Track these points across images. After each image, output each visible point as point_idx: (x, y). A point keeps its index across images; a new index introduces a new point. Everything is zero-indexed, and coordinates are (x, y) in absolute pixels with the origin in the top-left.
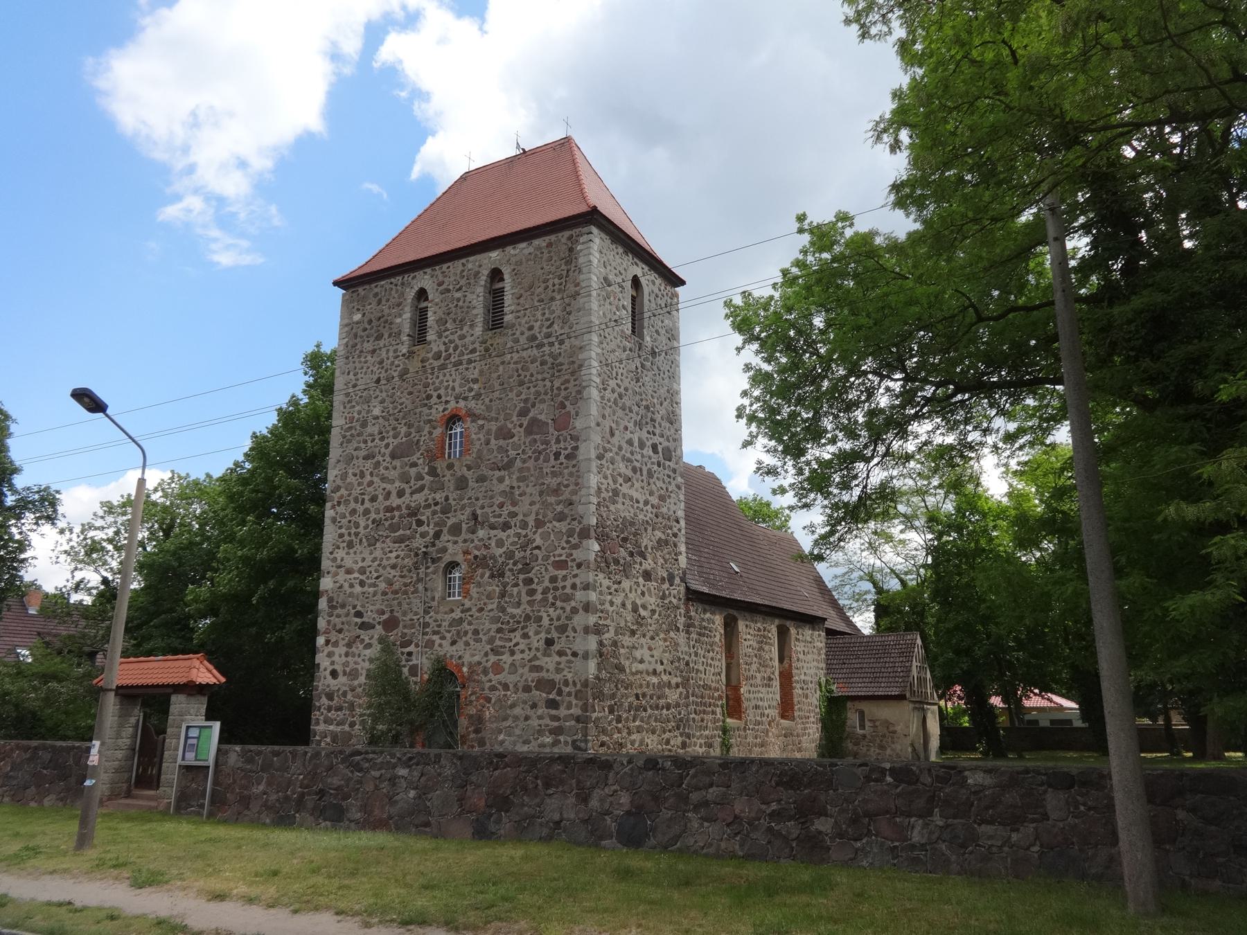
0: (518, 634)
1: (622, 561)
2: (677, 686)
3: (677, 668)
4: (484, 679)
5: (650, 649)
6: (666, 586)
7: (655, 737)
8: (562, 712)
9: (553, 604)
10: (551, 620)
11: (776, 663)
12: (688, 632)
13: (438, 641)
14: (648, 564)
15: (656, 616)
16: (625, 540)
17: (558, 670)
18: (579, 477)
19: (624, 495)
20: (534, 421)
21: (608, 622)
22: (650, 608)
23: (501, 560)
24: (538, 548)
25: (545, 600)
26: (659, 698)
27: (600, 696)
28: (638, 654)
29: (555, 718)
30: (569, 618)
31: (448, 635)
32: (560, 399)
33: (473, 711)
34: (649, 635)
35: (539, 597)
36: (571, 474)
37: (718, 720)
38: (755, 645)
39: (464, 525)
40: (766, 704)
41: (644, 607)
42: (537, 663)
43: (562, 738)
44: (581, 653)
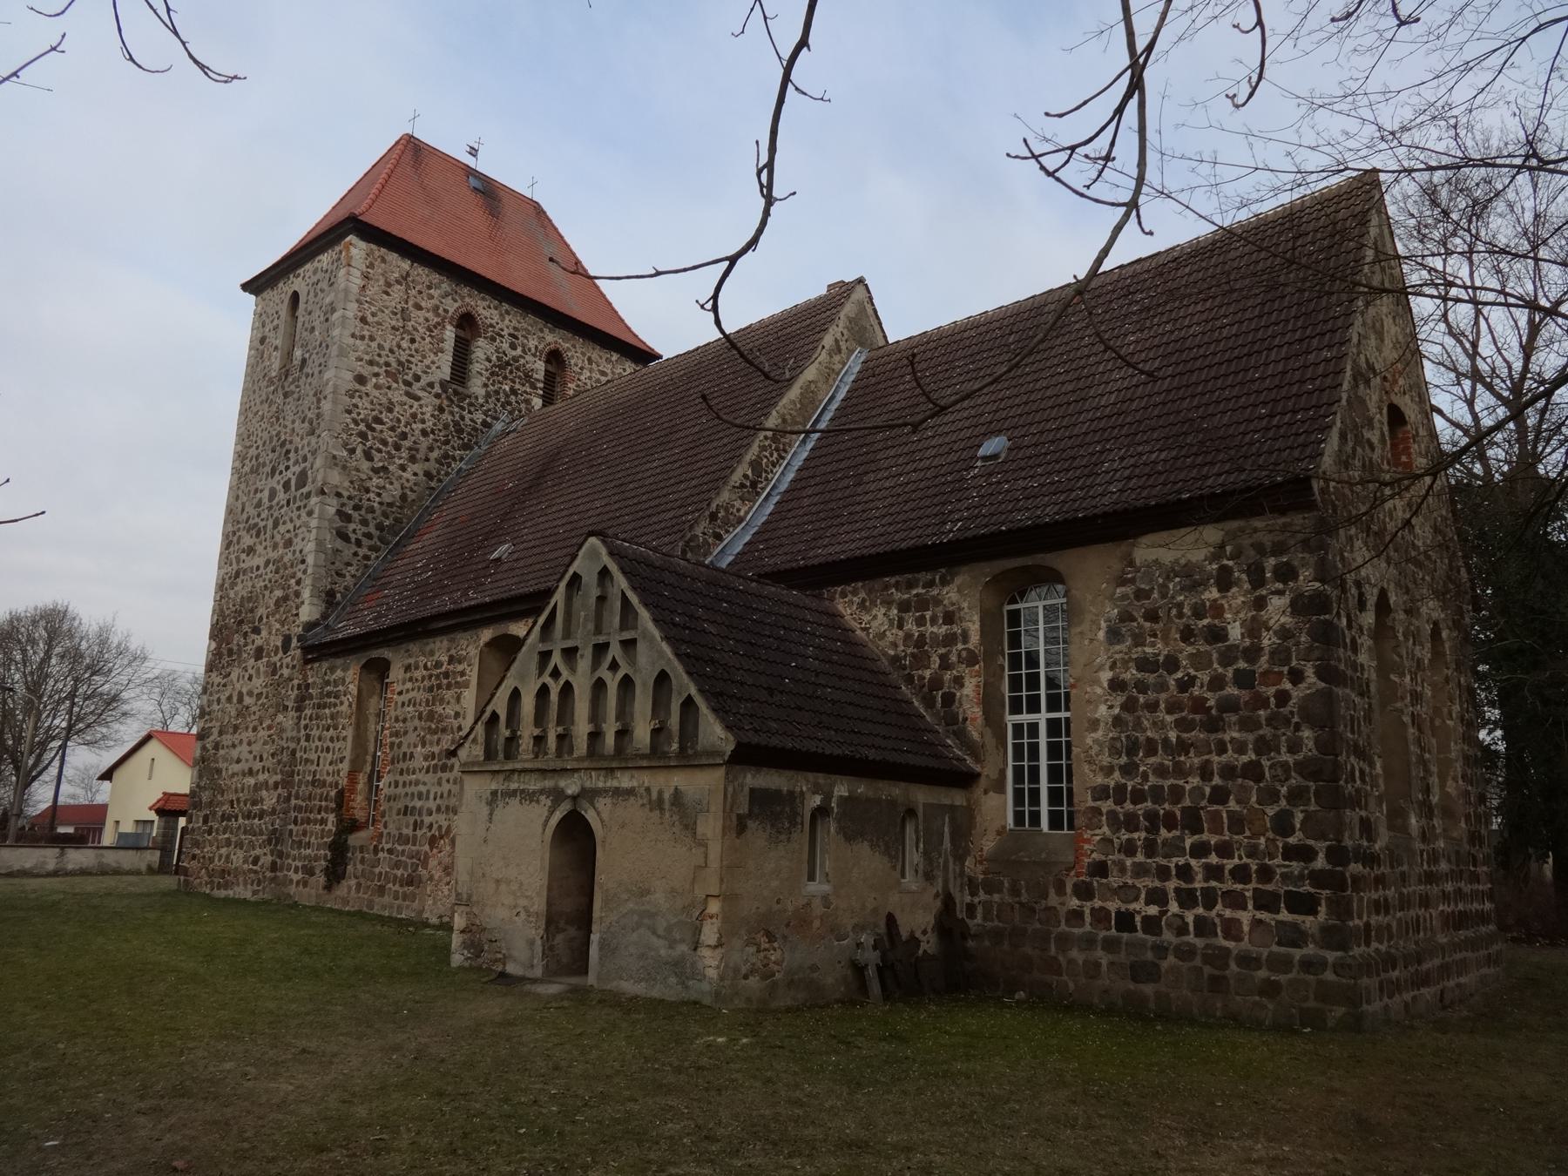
7: (241, 854)
15: (263, 700)
26: (254, 803)
38: (420, 696)
40: (432, 805)
41: (250, 693)
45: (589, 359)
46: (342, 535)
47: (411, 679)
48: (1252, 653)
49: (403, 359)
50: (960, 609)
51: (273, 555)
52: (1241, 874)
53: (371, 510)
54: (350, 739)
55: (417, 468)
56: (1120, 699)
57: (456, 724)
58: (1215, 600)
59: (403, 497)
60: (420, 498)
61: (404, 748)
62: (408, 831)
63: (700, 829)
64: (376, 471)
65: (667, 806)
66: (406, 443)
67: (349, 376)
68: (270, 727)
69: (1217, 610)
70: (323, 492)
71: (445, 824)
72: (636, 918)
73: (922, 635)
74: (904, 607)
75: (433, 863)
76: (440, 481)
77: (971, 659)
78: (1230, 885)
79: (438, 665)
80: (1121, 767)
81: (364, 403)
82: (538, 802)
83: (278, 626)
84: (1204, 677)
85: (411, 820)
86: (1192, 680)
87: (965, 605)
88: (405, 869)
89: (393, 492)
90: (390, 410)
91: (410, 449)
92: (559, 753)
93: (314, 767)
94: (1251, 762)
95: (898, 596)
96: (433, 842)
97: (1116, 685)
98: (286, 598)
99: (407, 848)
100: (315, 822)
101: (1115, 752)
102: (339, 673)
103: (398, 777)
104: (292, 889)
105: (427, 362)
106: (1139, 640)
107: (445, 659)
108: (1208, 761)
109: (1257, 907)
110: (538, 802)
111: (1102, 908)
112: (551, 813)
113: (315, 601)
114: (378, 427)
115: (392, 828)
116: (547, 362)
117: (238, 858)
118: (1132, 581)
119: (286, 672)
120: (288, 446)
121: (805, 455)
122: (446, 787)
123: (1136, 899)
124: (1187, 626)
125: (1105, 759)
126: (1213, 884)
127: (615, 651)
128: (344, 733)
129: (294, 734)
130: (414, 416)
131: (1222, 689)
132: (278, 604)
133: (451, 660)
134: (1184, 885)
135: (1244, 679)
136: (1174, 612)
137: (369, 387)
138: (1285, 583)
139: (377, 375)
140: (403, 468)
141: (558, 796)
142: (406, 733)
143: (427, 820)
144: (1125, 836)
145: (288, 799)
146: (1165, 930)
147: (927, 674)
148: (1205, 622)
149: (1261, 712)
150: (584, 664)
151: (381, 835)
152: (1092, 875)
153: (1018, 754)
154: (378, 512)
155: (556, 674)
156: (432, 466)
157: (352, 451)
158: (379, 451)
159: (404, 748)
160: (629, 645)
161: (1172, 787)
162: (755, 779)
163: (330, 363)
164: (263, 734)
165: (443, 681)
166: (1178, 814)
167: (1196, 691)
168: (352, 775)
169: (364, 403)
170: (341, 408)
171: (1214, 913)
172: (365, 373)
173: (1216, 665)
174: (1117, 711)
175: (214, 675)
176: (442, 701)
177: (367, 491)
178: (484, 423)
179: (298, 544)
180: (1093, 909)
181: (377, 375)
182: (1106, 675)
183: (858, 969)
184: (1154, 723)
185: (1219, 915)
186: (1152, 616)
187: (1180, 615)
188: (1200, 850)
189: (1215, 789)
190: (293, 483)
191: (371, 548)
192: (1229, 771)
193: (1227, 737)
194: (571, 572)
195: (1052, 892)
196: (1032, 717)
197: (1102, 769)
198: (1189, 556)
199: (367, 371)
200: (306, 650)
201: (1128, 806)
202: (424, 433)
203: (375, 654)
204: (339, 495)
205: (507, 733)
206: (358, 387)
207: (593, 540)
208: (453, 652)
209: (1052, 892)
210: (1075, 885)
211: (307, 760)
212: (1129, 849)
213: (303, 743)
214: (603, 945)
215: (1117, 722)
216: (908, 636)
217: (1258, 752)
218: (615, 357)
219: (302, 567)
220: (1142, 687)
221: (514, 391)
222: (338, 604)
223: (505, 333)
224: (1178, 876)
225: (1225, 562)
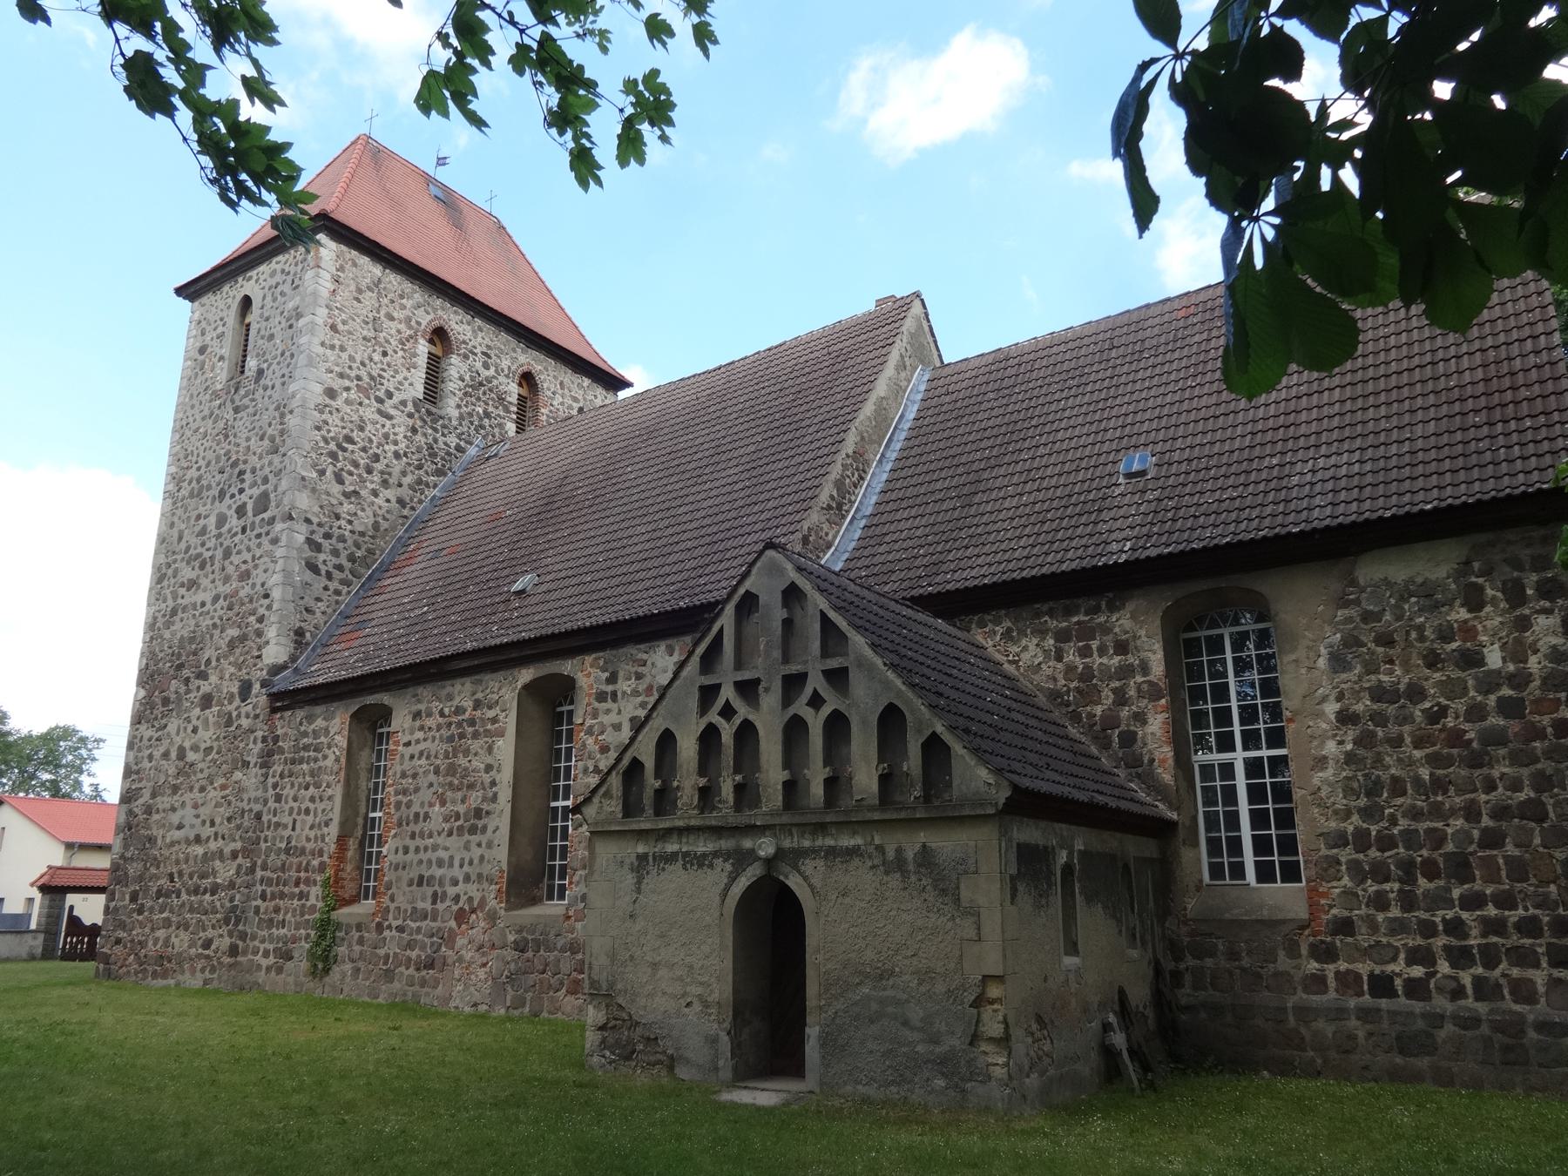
2: (234, 855)
7: (185, 936)
15: (213, 755)
26: (202, 877)
37: (313, 909)
40: (458, 873)
41: (195, 748)
45: (561, 383)
46: (312, 567)
47: (422, 728)
48: (1519, 680)
49: (374, 373)
50: (1135, 637)
51: (227, 589)
52: (1529, 927)
53: (342, 539)
54: (338, 800)
55: (390, 493)
56: (1351, 734)
57: (487, 778)
58: (1466, 622)
59: (376, 526)
60: (394, 528)
61: (416, 808)
62: (428, 905)
63: (965, 894)
64: (346, 495)
65: (911, 867)
66: (378, 466)
67: (319, 389)
68: (223, 787)
69: (1468, 631)
70: (291, 518)
71: (477, 896)
72: (874, 1006)
73: (1087, 667)
74: (1062, 637)
75: (461, 942)
76: (413, 509)
77: (1154, 693)
78: (1515, 940)
79: (459, 710)
80: (1360, 811)
81: (334, 420)
82: (711, 866)
83: (232, 670)
84: (1460, 705)
85: (429, 891)
86: (1443, 711)
87: (1143, 633)
88: (423, 948)
89: (365, 520)
90: (362, 429)
91: (382, 473)
92: (738, 807)
93: (287, 833)
94: (1529, 800)
95: (1053, 624)
96: (461, 917)
97: (1345, 718)
98: (243, 638)
99: (424, 924)
101: (1349, 791)
102: (320, 723)
103: (408, 842)
104: (261, 976)
105: (399, 377)
106: (1370, 668)
107: (468, 704)
108: (1473, 801)
109: (1555, 964)
110: (711, 866)
111: (1348, 971)
112: (733, 879)
113: (283, 640)
114: (350, 447)
115: (402, 901)
116: (520, 385)
117: (181, 941)
118: (1357, 602)
119: (245, 723)
120: (242, 466)
121: (885, 477)
123: (1394, 959)
124: (1433, 651)
125: (1340, 801)
126: (1495, 939)
127: (816, 682)
128: (330, 792)
129: (259, 793)
130: (386, 436)
131: (1483, 718)
132: (232, 645)
133: (477, 705)
134: (1455, 942)
135: (1510, 708)
136: (1414, 635)
137: (339, 402)
138: (1552, 601)
139: (347, 389)
140: (375, 493)
141: (741, 859)
142: (417, 790)
143: (452, 891)
144: (1372, 887)
145: (252, 870)
146: (1434, 994)
147: (1098, 710)
148: (1454, 645)
149: (1537, 744)
150: (770, 699)
151: (387, 910)
152: (1334, 933)
153: (1210, 800)
154: (350, 542)
155: (728, 712)
156: (405, 492)
157: (322, 473)
158: (351, 474)
159: (416, 808)
160: (837, 678)
161: (1429, 831)
162: (1030, 833)
163: (297, 374)
164: (213, 794)
165: (462, 732)
166: (1441, 861)
167: (1450, 722)
168: (342, 840)
169: (334, 420)
170: (309, 424)
171: (1497, 972)
172: (336, 387)
173: (1472, 693)
174: (1349, 747)
175: (143, 727)
176: (466, 752)
177: (338, 517)
178: (459, 449)
179: (258, 576)
180: (1337, 973)
181: (347, 389)
182: (1331, 708)
183: (1108, 1052)
184: (1400, 760)
185: (1504, 975)
186: (1386, 640)
187: (1422, 638)
188: (1473, 902)
189: (1485, 831)
190: (250, 507)
191: (343, 582)
192: (1501, 812)
193: (1496, 773)
194: (742, 591)
195: (1281, 954)
196: (1226, 756)
197: (1336, 812)
198: (1428, 575)
199: (337, 384)
200: (274, 697)
201: (1374, 853)
202: (397, 455)
203: (371, 699)
204: (308, 521)
205: (658, 784)
206: (328, 401)
207: (770, 553)
208: (480, 695)
209: (1281, 954)
210: (1312, 946)
211: (278, 825)
212: (1380, 902)
213: (272, 804)
214: (825, 1041)
215: (1350, 758)
216: (1070, 669)
217: (1539, 789)
218: (586, 382)
219: (267, 602)
220: (1379, 719)
221: (487, 415)
222: (308, 644)
223: (478, 351)
224: (1447, 932)
225: (1473, 579)
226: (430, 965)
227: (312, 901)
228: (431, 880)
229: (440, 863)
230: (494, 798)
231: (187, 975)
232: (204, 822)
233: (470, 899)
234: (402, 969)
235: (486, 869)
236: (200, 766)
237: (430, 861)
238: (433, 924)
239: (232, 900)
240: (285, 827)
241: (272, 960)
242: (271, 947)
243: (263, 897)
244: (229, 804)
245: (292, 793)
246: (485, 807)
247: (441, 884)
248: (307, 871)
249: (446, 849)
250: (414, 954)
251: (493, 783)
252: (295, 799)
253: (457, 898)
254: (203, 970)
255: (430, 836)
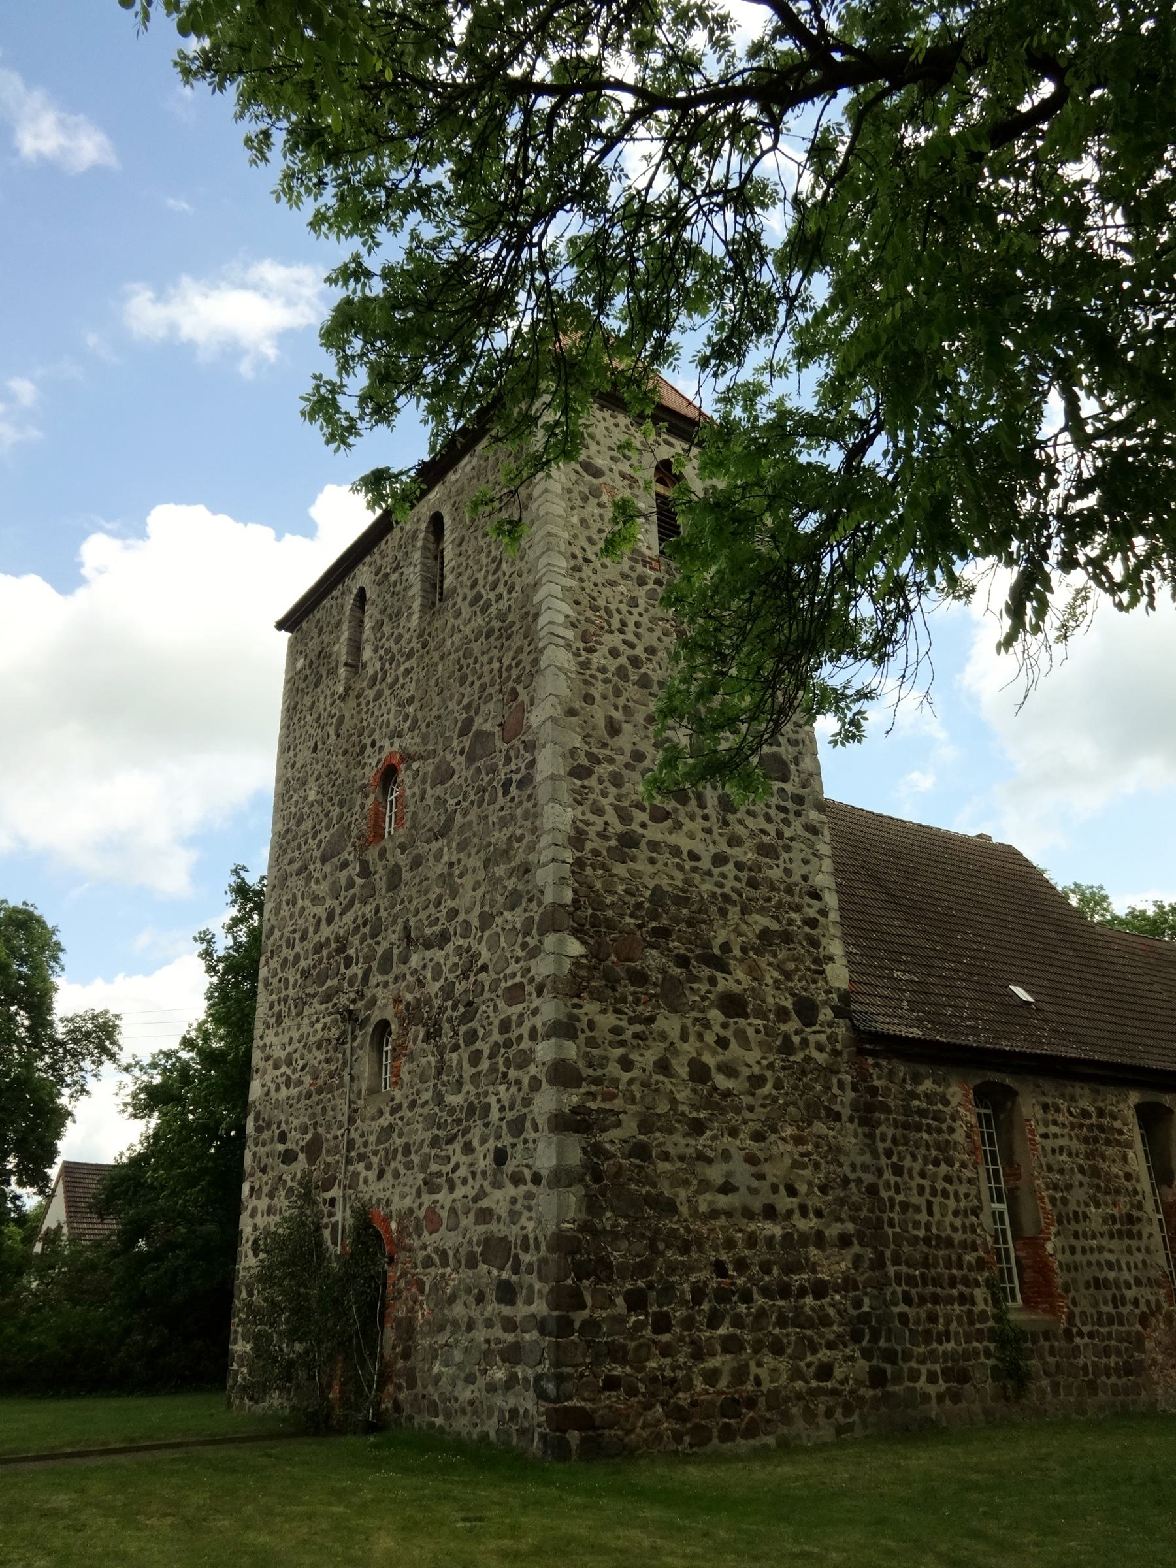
0: (458, 1145)
1: (655, 976)
2: (844, 1241)
3: (841, 1202)
4: (417, 1243)
5: (751, 1160)
6: (793, 1025)
7: (783, 1365)
8: (521, 1311)
9: (505, 1075)
10: (502, 1109)
11: (1145, 1183)
12: (864, 1122)
13: (364, 1173)
14: (737, 980)
15: (768, 1089)
16: (663, 933)
17: (514, 1216)
18: (536, 816)
19: (654, 846)
20: (480, 734)
21: (617, 1104)
22: (746, 1072)
23: (437, 1002)
24: (484, 968)
25: (493, 1069)
26: (789, 1269)
27: (603, 1270)
28: (715, 1173)
29: (509, 1325)
30: (527, 1102)
31: (375, 1160)
32: (511, 684)
33: (402, 1313)
34: (745, 1132)
35: (485, 1065)
36: (526, 815)
37: (983, 1316)
39: (396, 951)
40: (1126, 1275)
41: (729, 1070)
42: (484, 1203)
43: (519, 1371)
44: (545, 1173)
61: (1073, 1206)
62: (1108, 1309)
68: (799, 1140)
71: (1152, 1299)
75: (1149, 1344)
79: (1085, 1114)
85: (1109, 1294)
88: (1119, 1353)
96: (1144, 1320)
100: (950, 1300)
102: (927, 1085)
103: (1073, 1242)
104: (933, 1410)
122: (1139, 1257)
133: (1101, 1113)
142: (1069, 1187)
143: (1130, 1294)
145: (879, 1263)
159: (1073, 1206)
176: (1104, 1158)
203: (995, 1077)
213: (887, 1175)
226: (1128, 1372)
227: (981, 1306)
228: (1106, 1284)
229: (1110, 1266)
230: (1140, 1206)
231: (800, 1424)
232: (775, 1189)
233: (1148, 1302)
234: (1104, 1378)
235: (1155, 1274)
236: (746, 1100)
237: (1099, 1264)
238: (1122, 1329)
239: (858, 1304)
240: (918, 1209)
241: (942, 1386)
242: (937, 1368)
243: (908, 1300)
244: (817, 1166)
245: (917, 1167)
246: (1135, 1213)
247: (1118, 1288)
248: (960, 1268)
249: (1111, 1251)
250: (1112, 1361)
251: (1136, 1192)
252: (923, 1175)
253: (1136, 1303)
254: (829, 1413)
255: (1094, 1237)
